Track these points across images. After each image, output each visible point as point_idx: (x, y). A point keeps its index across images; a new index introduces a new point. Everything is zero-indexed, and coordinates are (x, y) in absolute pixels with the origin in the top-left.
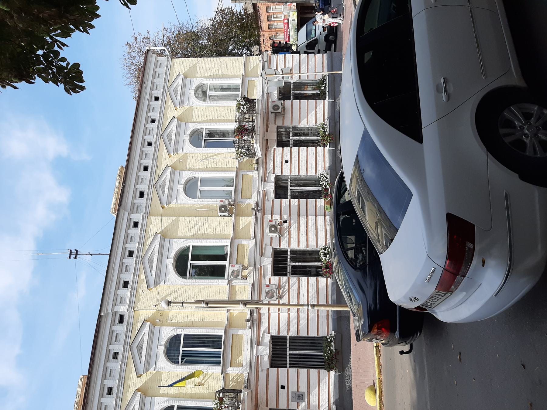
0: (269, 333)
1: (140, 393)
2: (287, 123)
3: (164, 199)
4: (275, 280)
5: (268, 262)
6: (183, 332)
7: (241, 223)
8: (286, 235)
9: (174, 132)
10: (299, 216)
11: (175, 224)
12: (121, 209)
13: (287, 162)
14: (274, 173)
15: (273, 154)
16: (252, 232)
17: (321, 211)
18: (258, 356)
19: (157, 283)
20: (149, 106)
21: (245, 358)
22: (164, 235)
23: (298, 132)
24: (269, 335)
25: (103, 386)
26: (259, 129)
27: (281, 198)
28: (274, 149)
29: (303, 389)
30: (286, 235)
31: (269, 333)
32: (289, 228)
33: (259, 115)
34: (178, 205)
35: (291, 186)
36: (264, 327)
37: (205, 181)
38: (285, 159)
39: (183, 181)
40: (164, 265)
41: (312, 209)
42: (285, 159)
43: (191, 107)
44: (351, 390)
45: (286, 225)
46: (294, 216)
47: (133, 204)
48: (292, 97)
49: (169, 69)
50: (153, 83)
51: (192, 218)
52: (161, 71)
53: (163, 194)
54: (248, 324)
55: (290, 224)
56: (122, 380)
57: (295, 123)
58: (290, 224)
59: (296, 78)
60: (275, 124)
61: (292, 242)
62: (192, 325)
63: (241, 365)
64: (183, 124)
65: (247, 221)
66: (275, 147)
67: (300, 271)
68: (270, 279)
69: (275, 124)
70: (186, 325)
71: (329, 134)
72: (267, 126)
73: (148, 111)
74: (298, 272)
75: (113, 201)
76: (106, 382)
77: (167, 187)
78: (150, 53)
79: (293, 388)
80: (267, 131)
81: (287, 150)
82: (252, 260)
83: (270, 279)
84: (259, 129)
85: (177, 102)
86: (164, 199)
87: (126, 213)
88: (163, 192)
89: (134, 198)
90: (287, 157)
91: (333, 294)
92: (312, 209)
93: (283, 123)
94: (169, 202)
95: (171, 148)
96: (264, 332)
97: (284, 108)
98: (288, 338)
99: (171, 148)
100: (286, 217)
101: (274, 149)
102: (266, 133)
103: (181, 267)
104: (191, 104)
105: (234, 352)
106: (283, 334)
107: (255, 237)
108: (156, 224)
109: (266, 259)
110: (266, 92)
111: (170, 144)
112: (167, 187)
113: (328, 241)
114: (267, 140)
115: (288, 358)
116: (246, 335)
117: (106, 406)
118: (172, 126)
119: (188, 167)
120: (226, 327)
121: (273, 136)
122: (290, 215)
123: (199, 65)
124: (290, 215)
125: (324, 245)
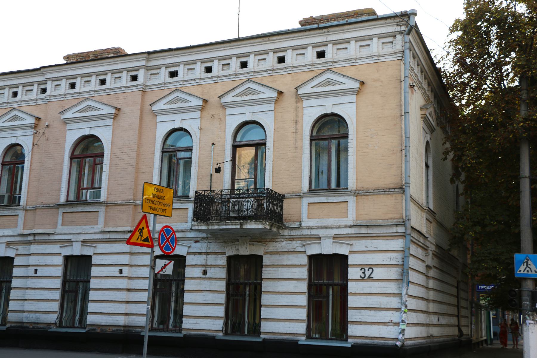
0: (17, 255)
10: (129, 290)
12: (146, 55)
14: (188, 253)
20: (304, 47)
36: (22, 249)
38: (209, 270)
40: (80, 125)
47: (158, 67)
50: (347, 41)
52: (375, 46)
59: (352, 287)
64: (273, 105)
77: (179, 105)
87: (143, 63)
90: (211, 272)
96: (17, 249)
105: (79, 214)
110: (321, 233)
111: (238, 95)
114: (238, 240)
122: (130, 278)
124: (130, 278)
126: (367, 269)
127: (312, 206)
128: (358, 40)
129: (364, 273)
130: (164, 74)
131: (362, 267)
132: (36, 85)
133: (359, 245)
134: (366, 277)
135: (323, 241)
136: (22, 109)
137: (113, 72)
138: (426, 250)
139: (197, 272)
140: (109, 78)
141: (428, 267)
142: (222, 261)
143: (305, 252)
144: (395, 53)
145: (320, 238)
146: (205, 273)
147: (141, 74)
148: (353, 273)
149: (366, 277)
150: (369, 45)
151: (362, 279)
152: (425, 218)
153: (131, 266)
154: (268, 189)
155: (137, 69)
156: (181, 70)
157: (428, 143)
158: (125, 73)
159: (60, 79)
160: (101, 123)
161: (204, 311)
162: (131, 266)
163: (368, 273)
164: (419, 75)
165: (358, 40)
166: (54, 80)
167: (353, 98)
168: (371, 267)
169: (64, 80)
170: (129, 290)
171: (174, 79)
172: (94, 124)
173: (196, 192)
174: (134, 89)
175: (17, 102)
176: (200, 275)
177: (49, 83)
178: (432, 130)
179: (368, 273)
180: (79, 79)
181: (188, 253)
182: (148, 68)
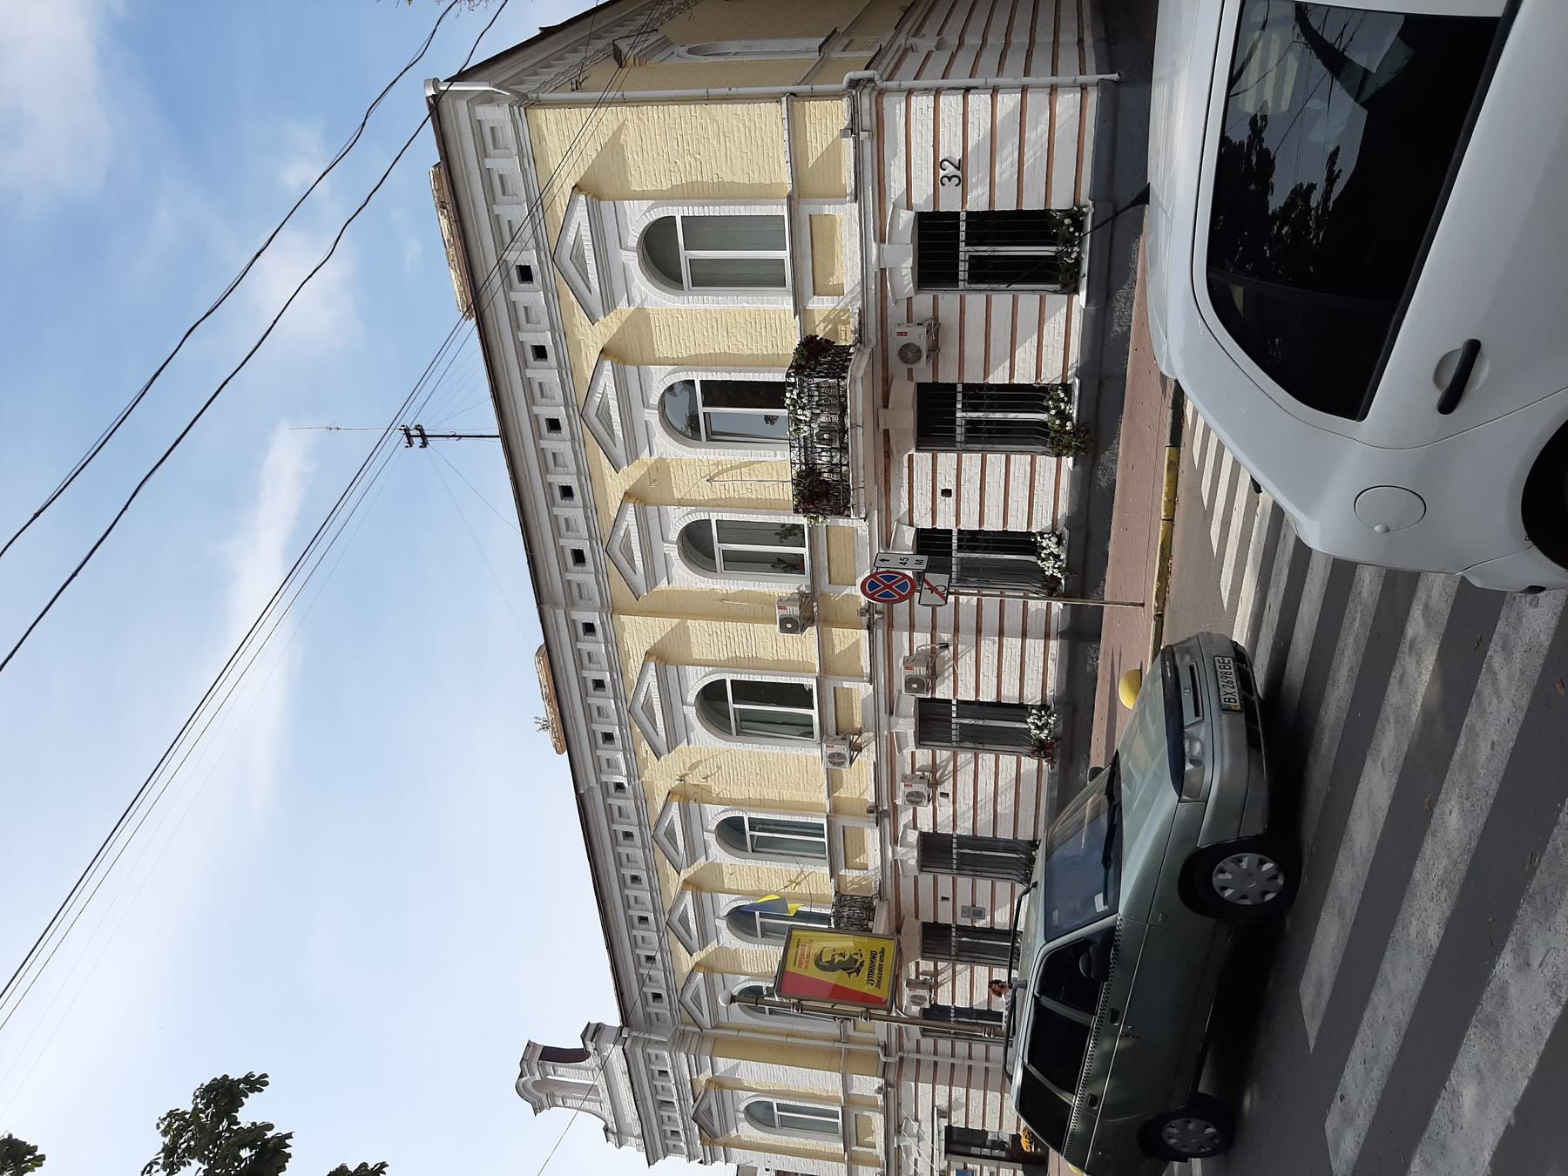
0: (915, 828)
1: (582, 198)
2: (948, 376)
3: (639, 578)
4: (924, 757)
5: (906, 726)
6: (698, 377)
7: (836, 642)
8: (949, 672)
9: (613, 404)
10: (979, 631)
11: (682, 634)
12: (545, 607)
13: (947, 493)
14: (911, 524)
15: (906, 470)
16: (848, 181)
17: (1036, 624)
18: (883, 271)
19: (672, 745)
21: (847, 269)
22: (659, 656)
23: (981, 395)
24: (911, 214)
25: (560, 550)
26: (861, 472)
27: (936, 386)
28: (911, 457)
29: (983, 902)
30: (949, 672)
31: (915, 828)
32: (955, 658)
33: (860, 431)
34: (676, 585)
35: (960, 548)
37: (730, 531)
38: (940, 487)
39: (633, 238)
41: (1013, 620)
42: (940, 487)
43: (640, 310)
44: (1125, 338)
45: (948, 654)
46: (967, 637)
48: (962, 275)
49: (530, 157)
51: (715, 625)
52: (506, 165)
53: (676, 850)
54: (865, 619)
55: (956, 650)
56: (560, 330)
57: (973, 376)
58: (956, 650)
59: (978, 201)
60: (910, 378)
61: (964, 683)
62: (761, 804)
63: (838, 291)
65: (852, 640)
66: (913, 451)
67: (990, 397)
68: (913, 754)
69: (910, 378)
70: (696, 362)
71: (1076, 429)
72: (886, 383)
73: (516, 327)
74: (978, 739)
75: (453, 283)
76: (522, 336)
78: (446, 103)
79: (964, 900)
80: (886, 406)
81: (947, 460)
82: (871, 721)
83: (913, 754)
84: (861, 472)
85: (595, 300)
86: (639, 578)
87: (560, 613)
88: (612, 434)
89: (564, 569)
90: (946, 481)
91: (1050, 789)
92: (1013, 620)
93: (935, 372)
94: (651, 579)
95: (620, 451)
96: (905, 826)
97: (934, 327)
98: (963, 216)
99: (620, 451)
100: (946, 637)
101: (911, 457)
102: (882, 412)
103: (658, 248)
104: (638, 300)
106: (945, 829)
107: (857, 195)
108: (639, 634)
109: (901, 721)
112: (617, 428)
113: (1050, 693)
114: (886, 432)
115: (959, 396)
116: (845, 218)
117: (492, 129)
118: (602, 383)
119: (677, 495)
120: (790, 197)
121: (905, 417)
122: (957, 629)
123: (630, 140)
124: (957, 629)
125: (1039, 697)
126: (942, 173)
127: (818, 289)
128: (491, 200)
129: (950, 179)
130: (576, 575)
131: (937, 182)
132: (610, 801)
133: (896, 187)
134: (959, 173)
135: (886, 265)
136: (653, 823)
137: (579, 666)
138: (906, 50)
139: (946, 506)
140: (591, 675)
141: (940, 46)
142: (923, 459)
143: (909, 299)
144: (514, 121)
145: (883, 271)
146: (947, 493)
147: (583, 617)
148: (950, 202)
149: (959, 173)
150: (501, 177)
151: (963, 181)
152: (843, 55)
153: (934, 628)
154: (788, 376)
155: (572, 623)
156: (571, 544)
157: (690, 51)
158: (580, 645)
159: (596, 760)
160: (674, 685)
161: (1021, 491)
162: (934, 628)
163: (950, 170)
164: (555, 70)
165: (491, 200)
166: (598, 770)
167: (607, 206)
168: (938, 165)
169: (599, 753)
170: (979, 631)
171: (587, 554)
172: (676, 700)
173: (796, 511)
174: (609, 628)
175: (641, 833)
176: (951, 500)
177: (604, 778)
178: (665, 43)
179: (950, 170)
180: (595, 726)
181: (911, 524)
182: (571, 604)
